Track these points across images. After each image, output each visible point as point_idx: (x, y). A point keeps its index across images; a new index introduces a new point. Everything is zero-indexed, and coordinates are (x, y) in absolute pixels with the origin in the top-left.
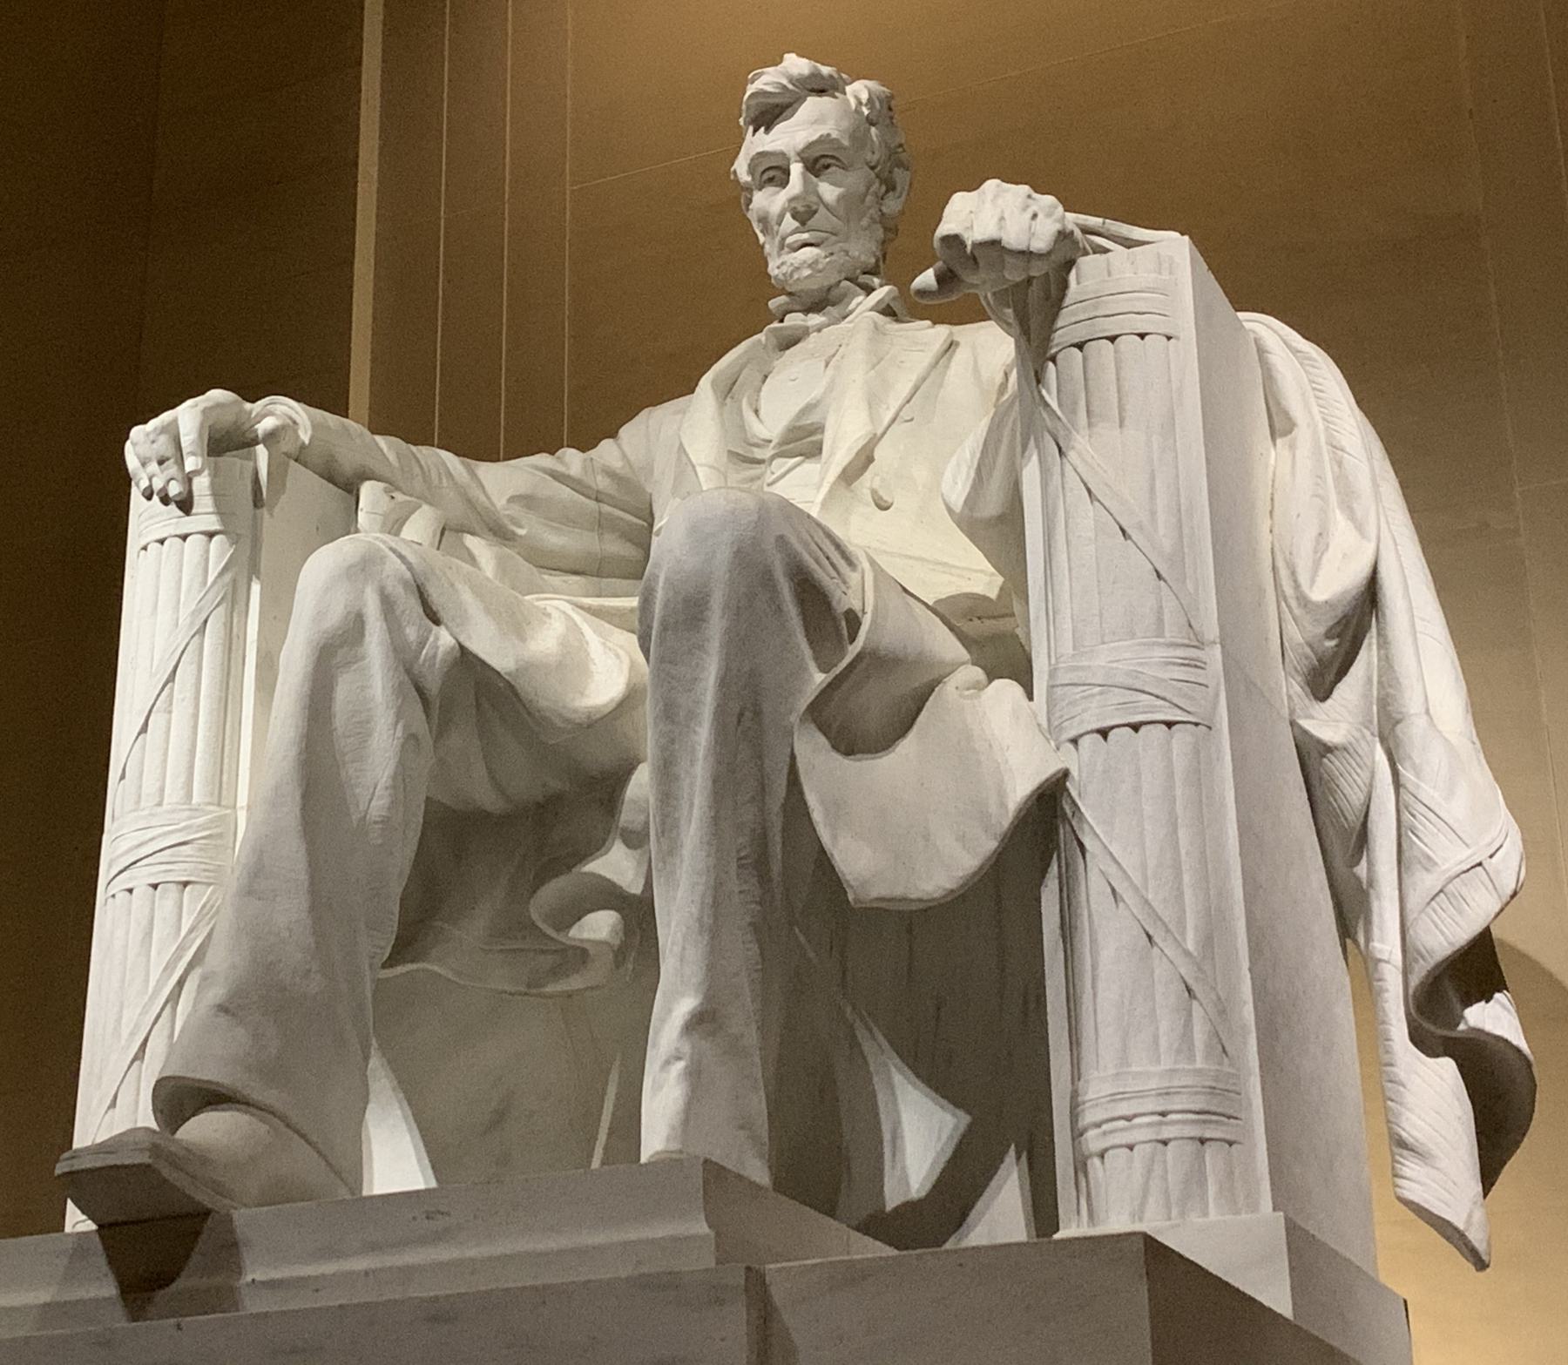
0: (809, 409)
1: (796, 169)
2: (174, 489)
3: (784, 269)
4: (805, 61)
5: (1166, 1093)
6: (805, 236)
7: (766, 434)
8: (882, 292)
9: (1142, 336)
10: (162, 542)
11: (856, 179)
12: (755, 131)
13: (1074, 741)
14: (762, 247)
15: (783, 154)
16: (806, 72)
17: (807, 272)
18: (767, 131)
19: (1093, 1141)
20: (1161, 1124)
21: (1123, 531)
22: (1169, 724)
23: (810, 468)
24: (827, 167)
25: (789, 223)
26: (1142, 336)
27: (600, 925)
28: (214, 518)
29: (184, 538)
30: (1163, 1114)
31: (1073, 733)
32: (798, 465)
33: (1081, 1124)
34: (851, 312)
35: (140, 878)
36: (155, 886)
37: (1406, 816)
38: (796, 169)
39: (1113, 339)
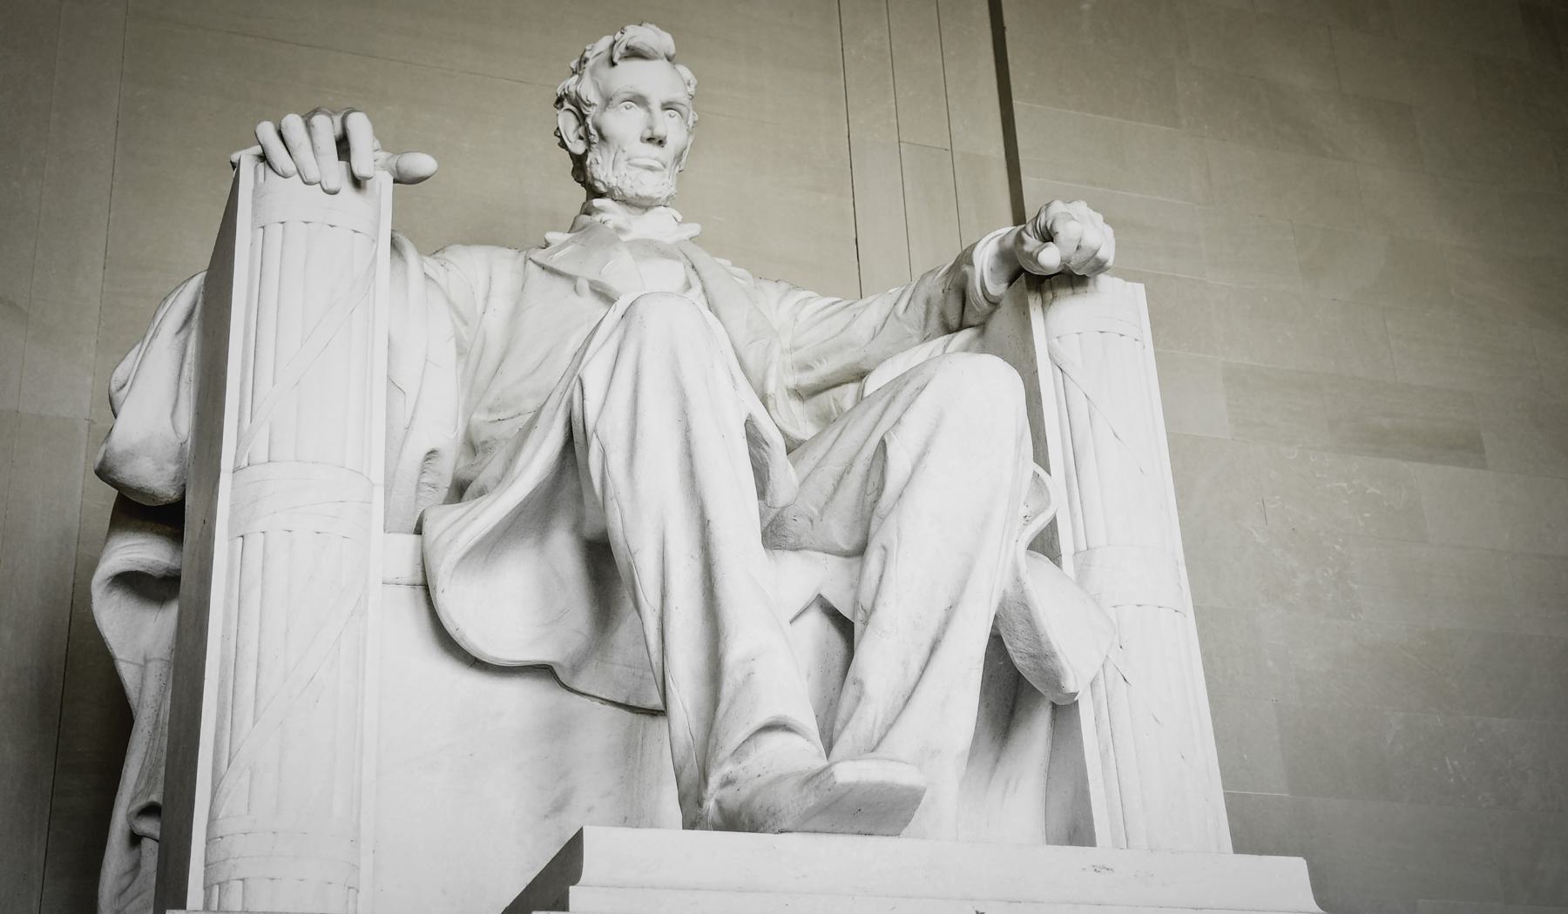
2: (332, 186)
8: (694, 229)
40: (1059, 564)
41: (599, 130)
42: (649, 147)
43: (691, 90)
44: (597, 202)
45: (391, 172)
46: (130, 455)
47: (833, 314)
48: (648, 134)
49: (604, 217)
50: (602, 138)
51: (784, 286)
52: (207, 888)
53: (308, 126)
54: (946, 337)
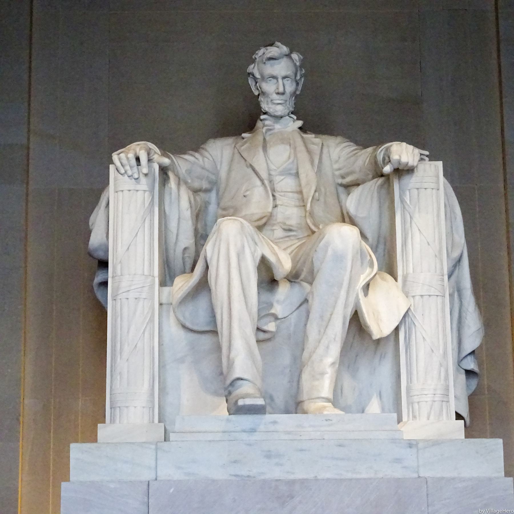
1: (280, 80)
2: (136, 176)
5: (435, 390)
8: (300, 123)
10: (129, 190)
11: (294, 84)
18: (272, 66)
19: (416, 399)
20: (434, 397)
21: (428, 243)
25: (275, 96)
28: (146, 186)
29: (137, 191)
30: (435, 394)
31: (413, 295)
33: (411, 394)
35: (132, 295)
36: (136, 298)
37: (464, 314)
39: (426, 189)
40: (396, 279)
41: (261, 88)
42: (279, 96)
43: (298, 64)
44: (262, 117)
45: (158, 163)
46: (96, 250)
47: (352, 156)
48: (277, 92)
49: (267, 122)
50: (262, 92)
51: (339, 139)
52: (111, 408)
53: (128, 158)
54: (376, 179)
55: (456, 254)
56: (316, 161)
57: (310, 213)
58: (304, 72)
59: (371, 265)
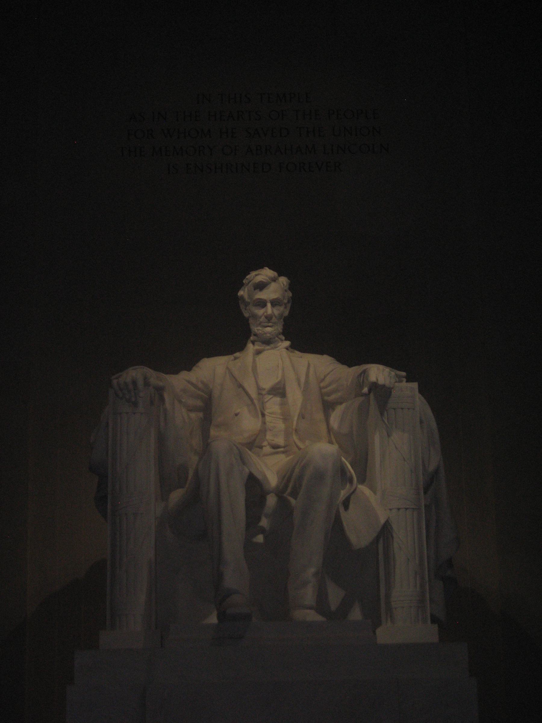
0: (279, 383)
1: (269, 305)
3: (261, 332)
4: (272, 272)
6: (270, 324)
7: (264, 387)
9: (409, 409)
12: (255, 290)
13: (391, 510)
14: (247, 320)
15: (265, 300)
16: (273, 276)
17: (268, 335)
22: (413, 509)
23: (278, 399)
24: (276, 305)
25: (263, 319)
26: (409, 409)
27: (260, 538)
32: (272, 398)
34: (277, 347)
38: (269, 305)
39: (402, 409)
44: (252, 338)
48: (265, 314)
55: (431, 468)
56: (303, 380)
57: (296, 430)
58: (290, 294)
59: (351, 481)
